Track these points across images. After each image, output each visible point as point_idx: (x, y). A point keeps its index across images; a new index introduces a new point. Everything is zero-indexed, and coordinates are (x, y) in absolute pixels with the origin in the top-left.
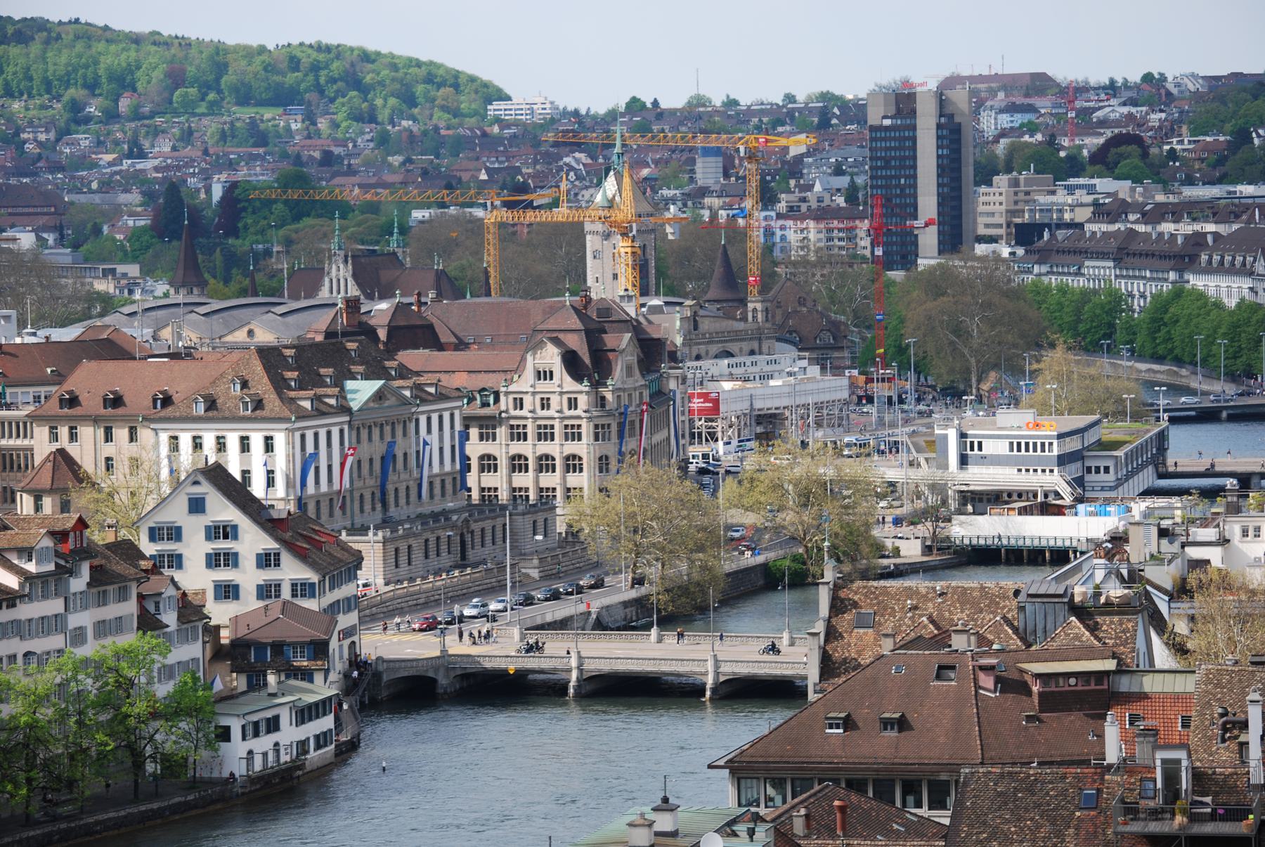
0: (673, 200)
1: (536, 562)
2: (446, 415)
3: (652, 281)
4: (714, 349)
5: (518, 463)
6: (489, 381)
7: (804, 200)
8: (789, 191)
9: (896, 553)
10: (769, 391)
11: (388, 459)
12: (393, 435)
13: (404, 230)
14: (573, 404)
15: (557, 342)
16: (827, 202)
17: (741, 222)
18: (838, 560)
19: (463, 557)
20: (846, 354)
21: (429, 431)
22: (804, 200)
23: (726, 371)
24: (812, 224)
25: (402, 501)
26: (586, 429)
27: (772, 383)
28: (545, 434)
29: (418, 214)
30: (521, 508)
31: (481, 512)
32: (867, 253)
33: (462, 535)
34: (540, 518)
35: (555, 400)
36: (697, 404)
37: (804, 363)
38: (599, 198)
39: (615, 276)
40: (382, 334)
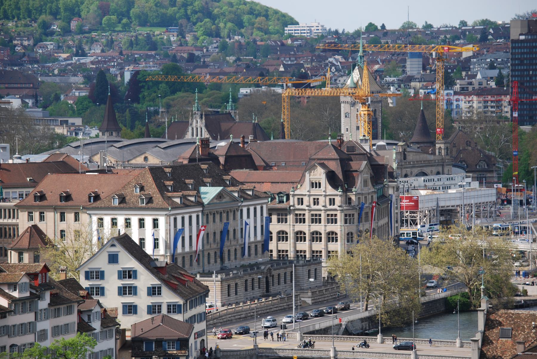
0: (393, 84)
1: (310, 294)
2: (258, 208)
3: (380, 130)
4: (416, 171)
5: (300, 236)
6: (284, 188)
7: (471, 84)
8: (461, 79)
9: (525, 293)
10: (448, 196)
11: (224, 233)
12: (228, 219)
13: (235, 100)
14: (332, 202)
15: (323, 166)
16: (484, 85)
17: (433, 96)
18: (490, 297)
19: (268, 290)
20: (495, 175)
21: (248, 217)
22: (471, 84)
23: (423, 184)
24: (475, 98)
25: (232, 257)
26: (340, 217)
27: (450, 191)
28: (316, 219)
29: (243, 91)
30: (301, 262)
31: (278, 264)
32: (509, 115)
33: (267, 278)
34: (312, 268)
35: (322, 200)
36: (405, 203)
37: (469, 180)
38: (349, 82)
39: (358, 128)
40: (222, 160)
